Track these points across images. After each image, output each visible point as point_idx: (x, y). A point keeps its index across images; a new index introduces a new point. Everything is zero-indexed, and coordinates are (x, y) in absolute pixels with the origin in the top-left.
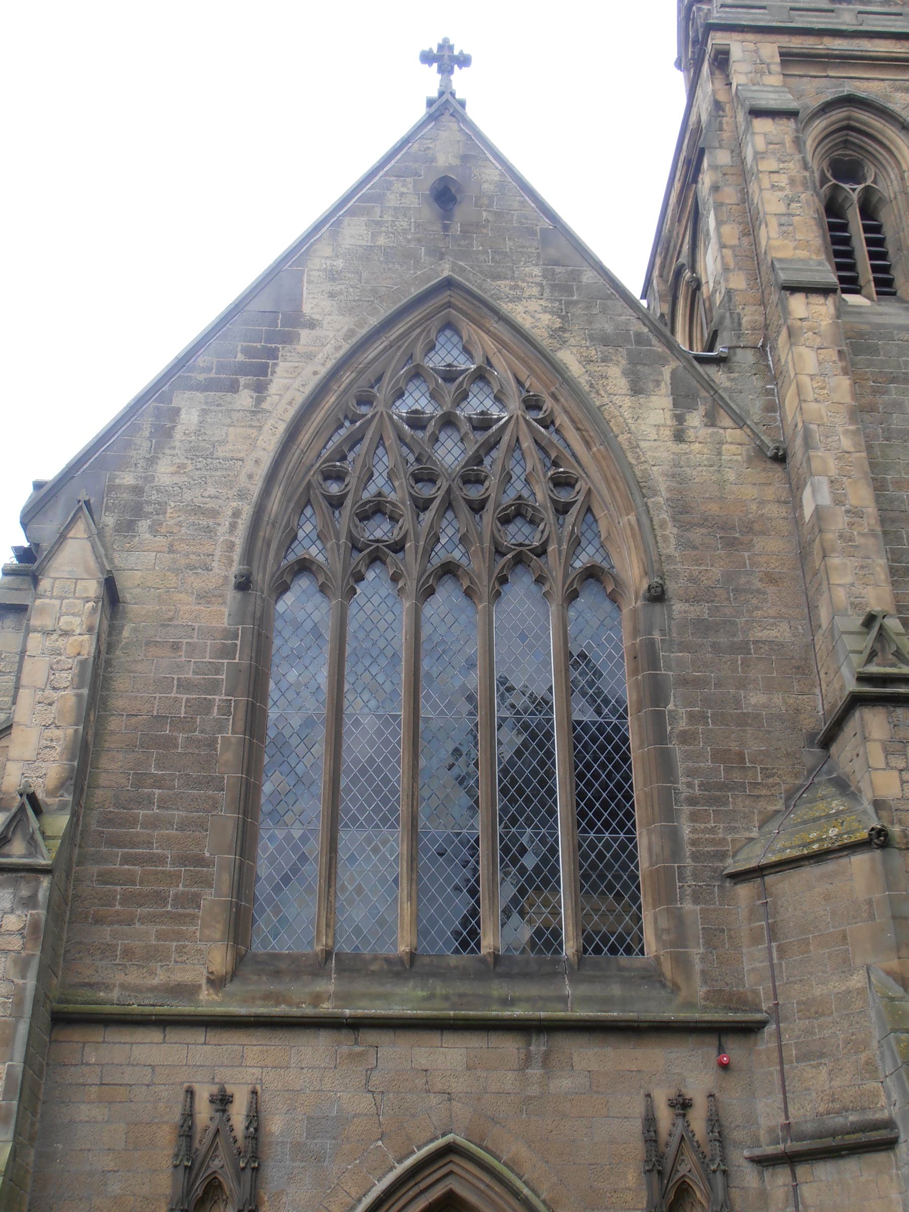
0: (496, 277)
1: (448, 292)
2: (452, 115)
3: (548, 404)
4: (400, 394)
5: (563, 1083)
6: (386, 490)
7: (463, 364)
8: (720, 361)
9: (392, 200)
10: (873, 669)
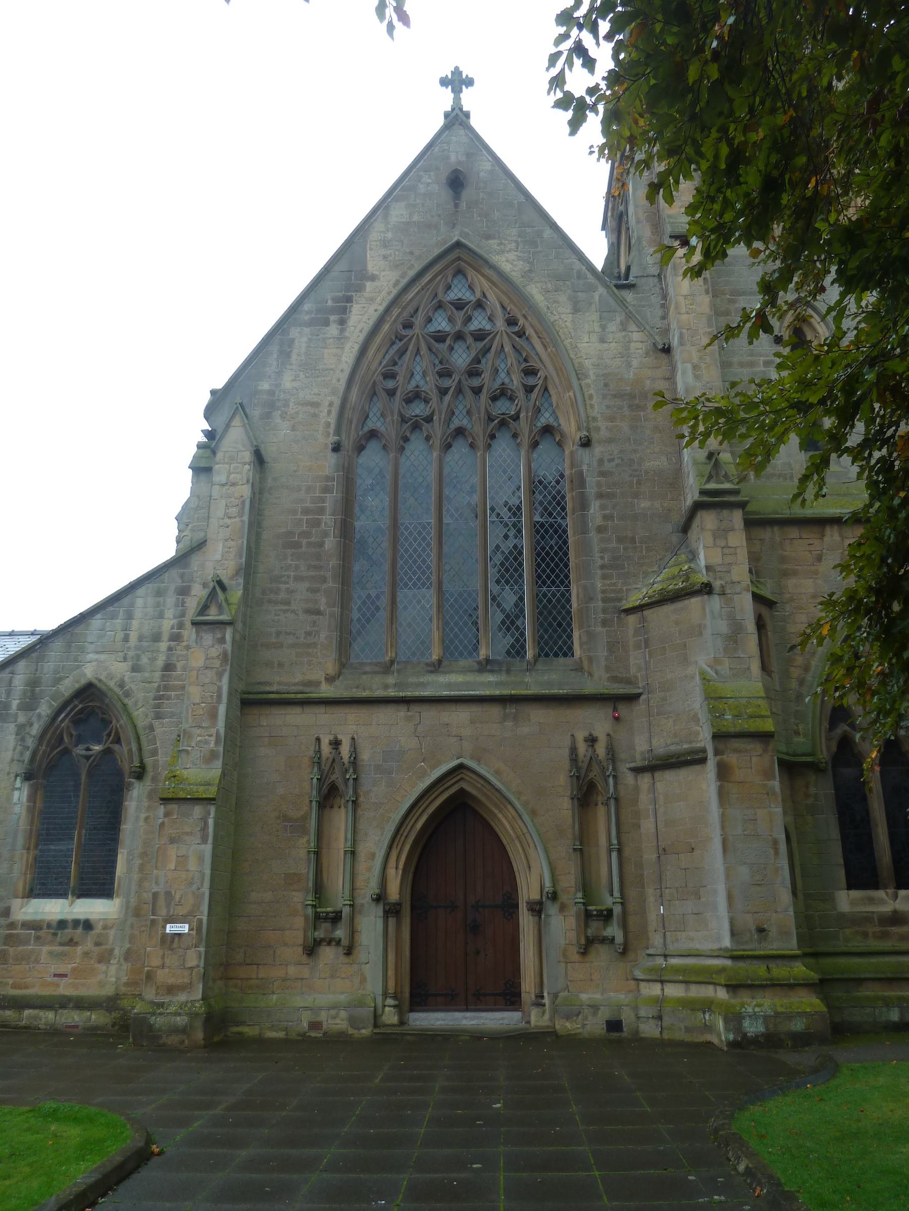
0: (488, 237)
1: (458, 251)
2: (460, 124)
3: (521, 322)
4: (429, 320)
6: (422, 383)
7: (467, 296)
8: (631, 287)
9: (422, 188)
10: (712, 486)
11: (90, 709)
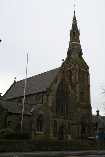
5: (66, 121)
11: (41, 116)
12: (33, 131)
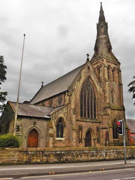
12: (50, 137)
